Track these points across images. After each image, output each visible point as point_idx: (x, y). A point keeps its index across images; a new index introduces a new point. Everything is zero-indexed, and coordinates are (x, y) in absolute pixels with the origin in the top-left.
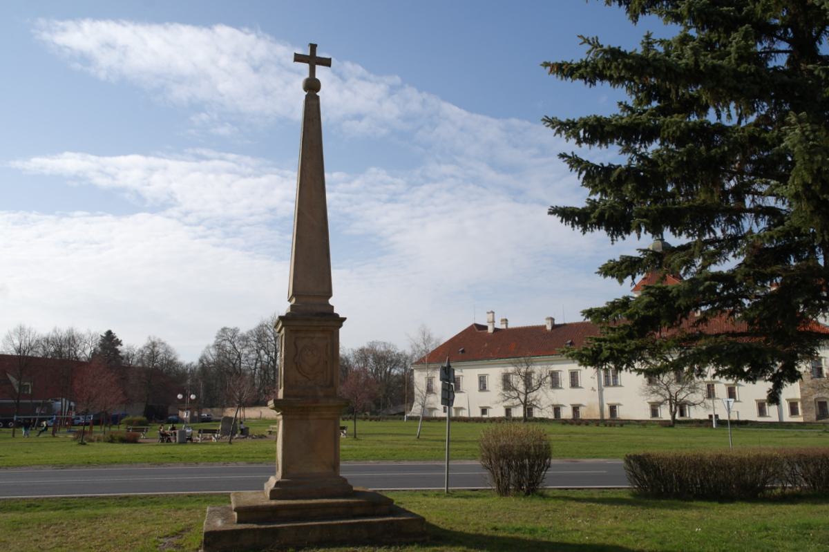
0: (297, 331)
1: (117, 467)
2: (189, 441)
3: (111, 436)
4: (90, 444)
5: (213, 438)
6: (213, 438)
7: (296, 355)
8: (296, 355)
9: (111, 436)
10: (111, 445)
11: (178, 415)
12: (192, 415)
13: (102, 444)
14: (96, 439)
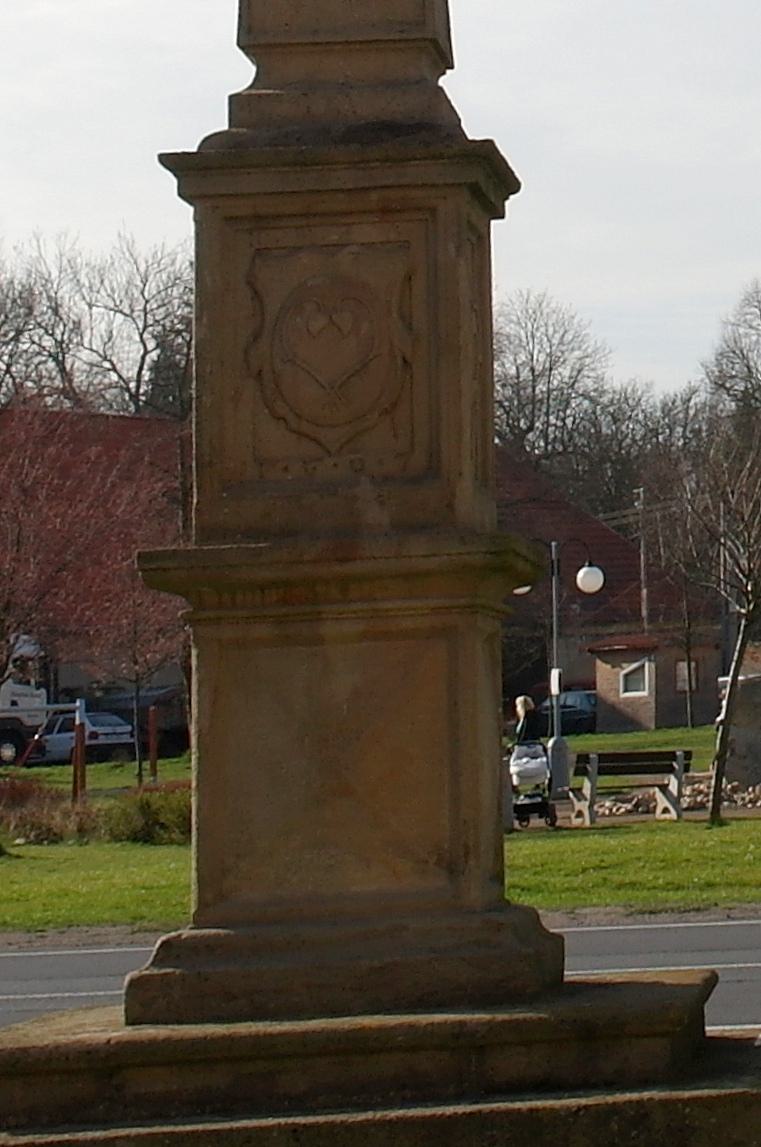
0: (259, 221)
1: (724, 1030)
2: (536, 822)
3: (145, 808)
4: (44, 850)
5: (662, 802)
6: (662, 802)
7: (256, 336)
8: (256, 336)
9: (145, 808)
10: (140, 852)
11: (592, 685)
12: (665, 680)
13: (100, 851)
14: (72, 826)
